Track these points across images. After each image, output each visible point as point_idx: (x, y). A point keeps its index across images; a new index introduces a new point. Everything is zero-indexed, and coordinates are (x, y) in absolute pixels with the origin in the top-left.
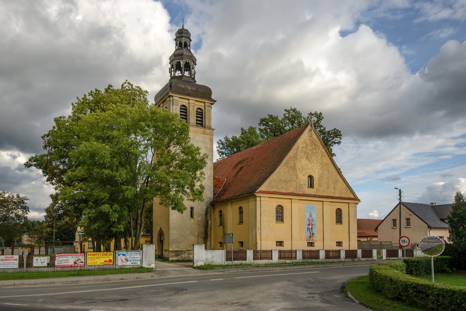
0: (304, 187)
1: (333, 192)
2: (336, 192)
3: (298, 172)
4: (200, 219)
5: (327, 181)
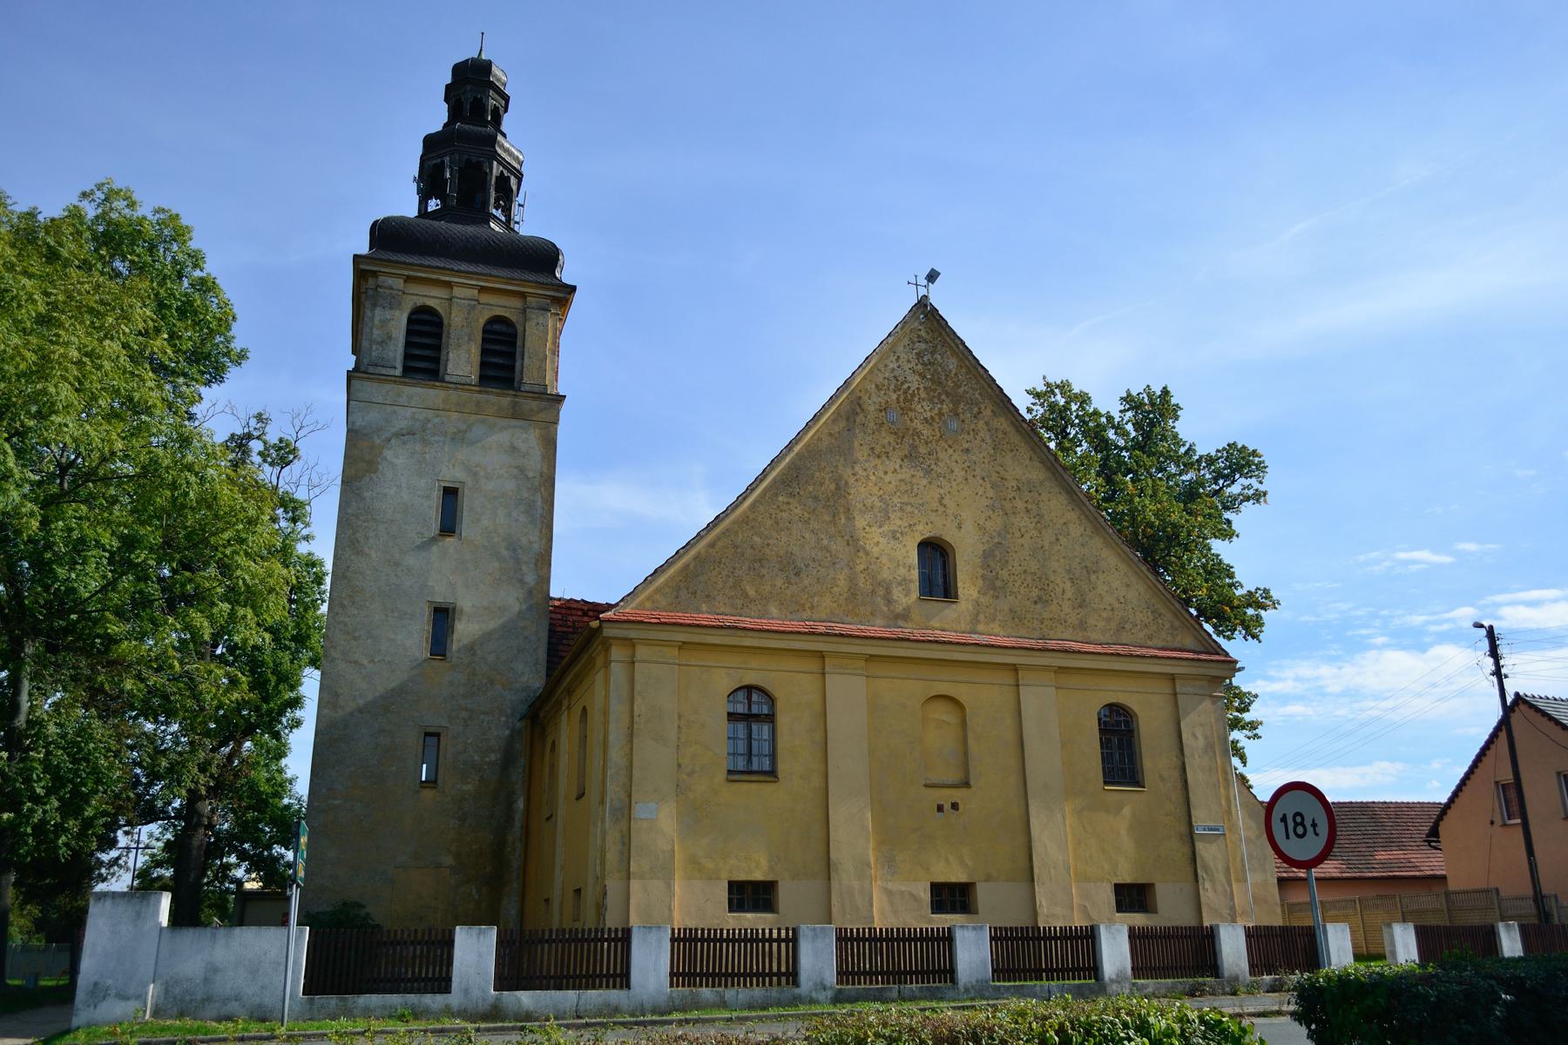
0: (897, 593)
1: (1073, 619)
2: (1091, 621)
3: (860, 522)
4: (468, 787)
5: (1033, 566)
